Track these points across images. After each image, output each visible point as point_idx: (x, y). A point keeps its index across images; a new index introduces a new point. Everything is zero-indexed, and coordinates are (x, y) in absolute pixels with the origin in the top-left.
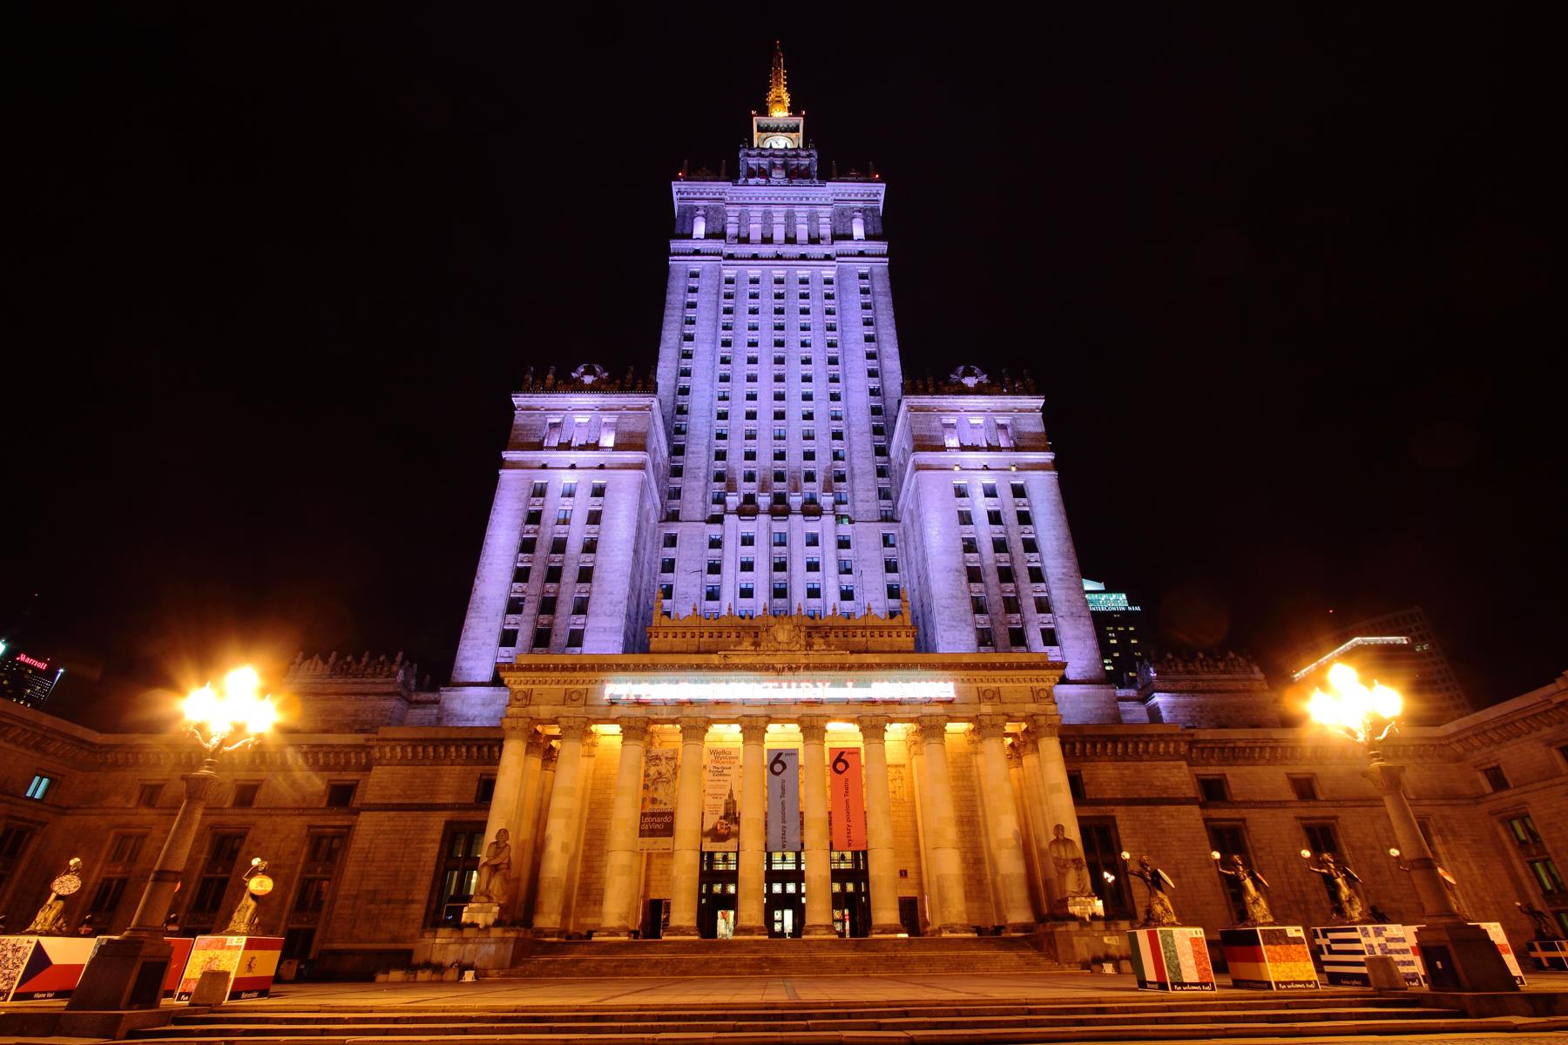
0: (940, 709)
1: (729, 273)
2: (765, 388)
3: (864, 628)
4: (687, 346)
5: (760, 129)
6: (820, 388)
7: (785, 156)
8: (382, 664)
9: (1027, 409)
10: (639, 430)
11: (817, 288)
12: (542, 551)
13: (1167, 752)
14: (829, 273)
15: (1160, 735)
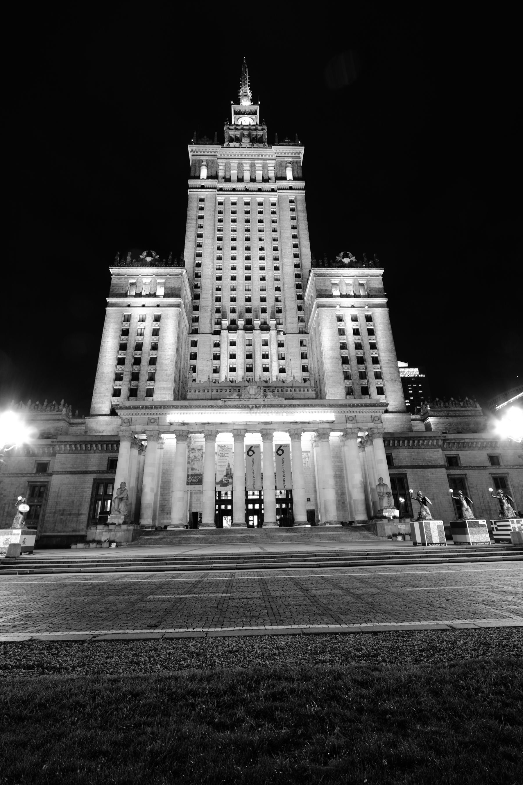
0: (327, 426)
1: (220, 199)
2: (240, 263)
3: (291, 387)
4: (200, 240)
5: (236, 113)
6: (268, 263)
7: (249, 129)
8: (54, 405)
9: (374, 275)
10: (176, 286)
11: (267, 208)
12: (131, 349)
13: (432, 444)
14: (274, 199)
15: (430, 437)
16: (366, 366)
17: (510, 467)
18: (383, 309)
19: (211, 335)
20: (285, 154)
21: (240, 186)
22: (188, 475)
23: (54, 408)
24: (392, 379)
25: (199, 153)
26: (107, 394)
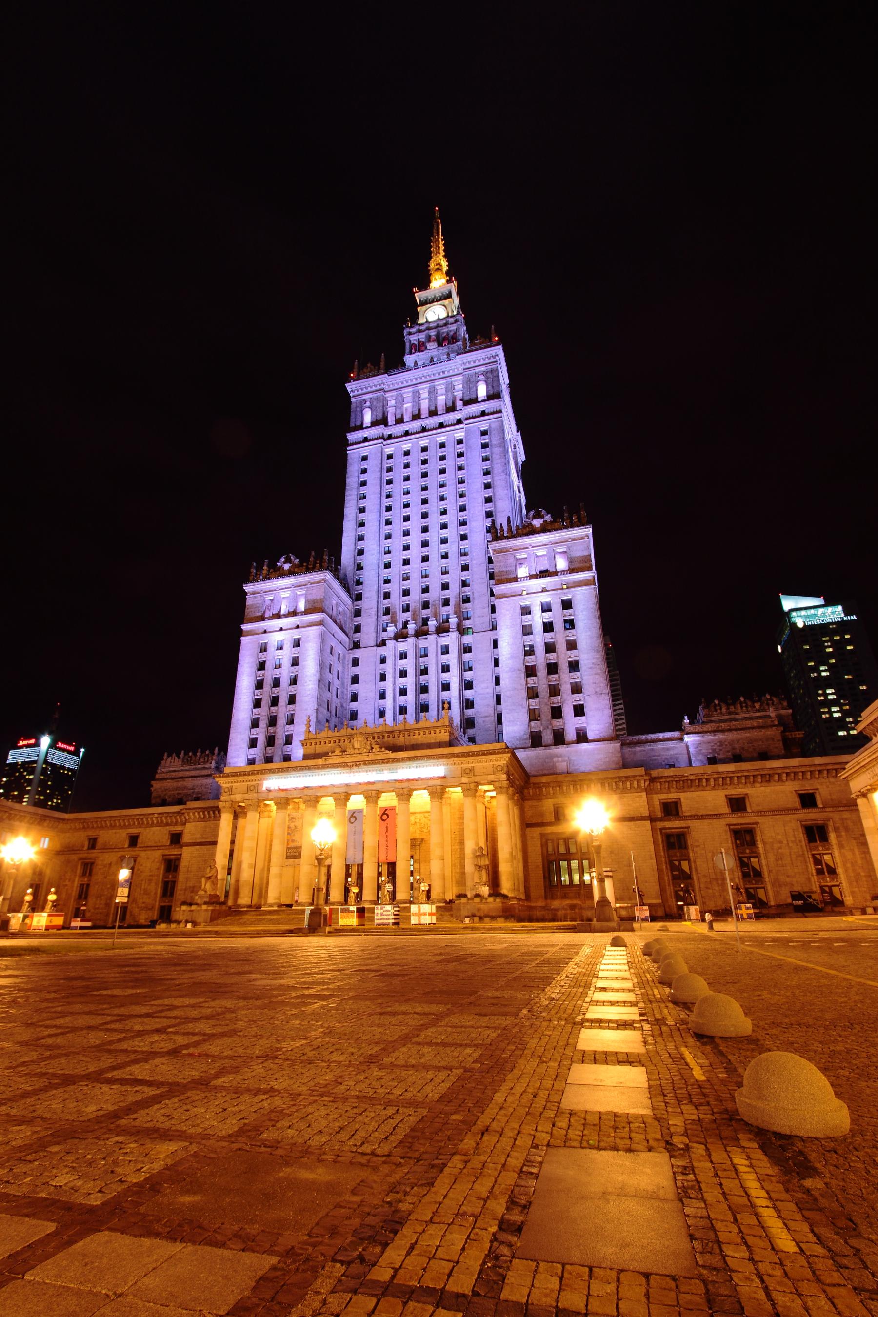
0: (438, 782)
1: (389, 450)
2: (414, 540)
6: (451, 533)
7: (438, 326)
8: (208, 755)
9: (581, 538)
10: (318, 597)
14: (460, 435)
15: (626, 777)
17: (761, 813)
18: (588, 587)
20: (474, 362)
21: (416, 425)
22: (288, 848)
25: (361, 392)
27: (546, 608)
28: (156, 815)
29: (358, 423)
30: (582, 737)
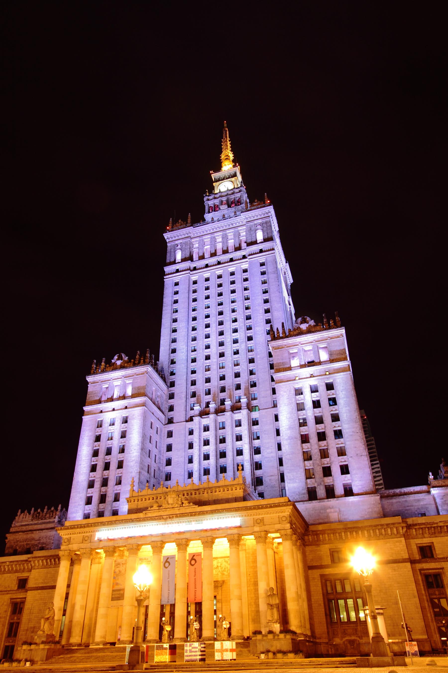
0: (235, 531)
1: (194, 278)
2: (213, 341)
6: (241, 335)
7: (227, 195)
8: (53, 511)
9: (338, 336)
15: (387, 525)
16: (327, 443)
18: (345, 373)
19: (185, 423)
20: (254, 217)
21: (214, 260)
22: (113, 591)
23: (53, 514)
24: (357, 455)
25: (174, 239)
26: (80, 503)
27: (314, 390)
28: (8, 563)
29: (172, 260)
30: (348, 492)
